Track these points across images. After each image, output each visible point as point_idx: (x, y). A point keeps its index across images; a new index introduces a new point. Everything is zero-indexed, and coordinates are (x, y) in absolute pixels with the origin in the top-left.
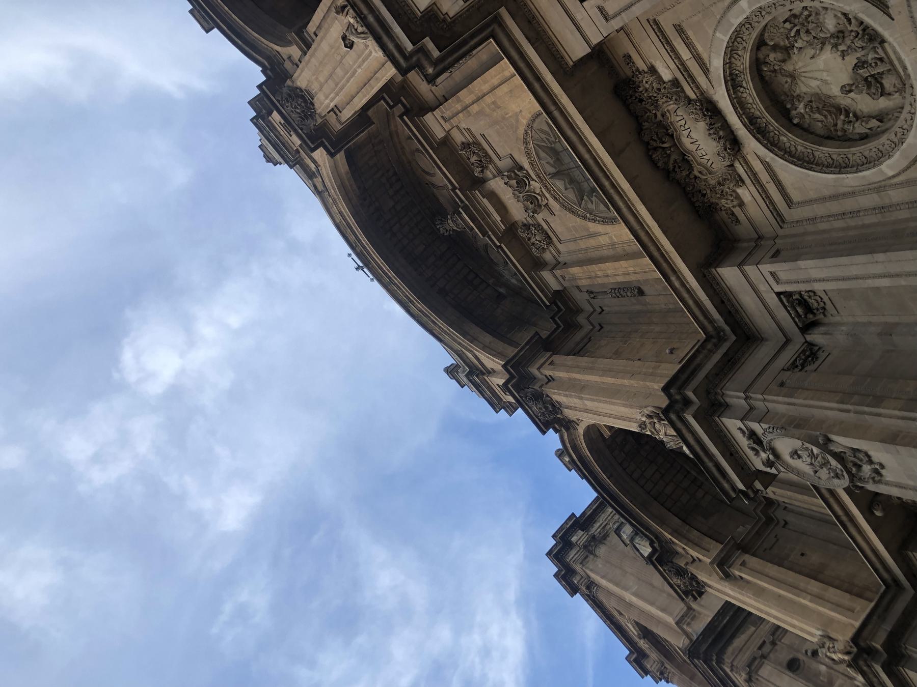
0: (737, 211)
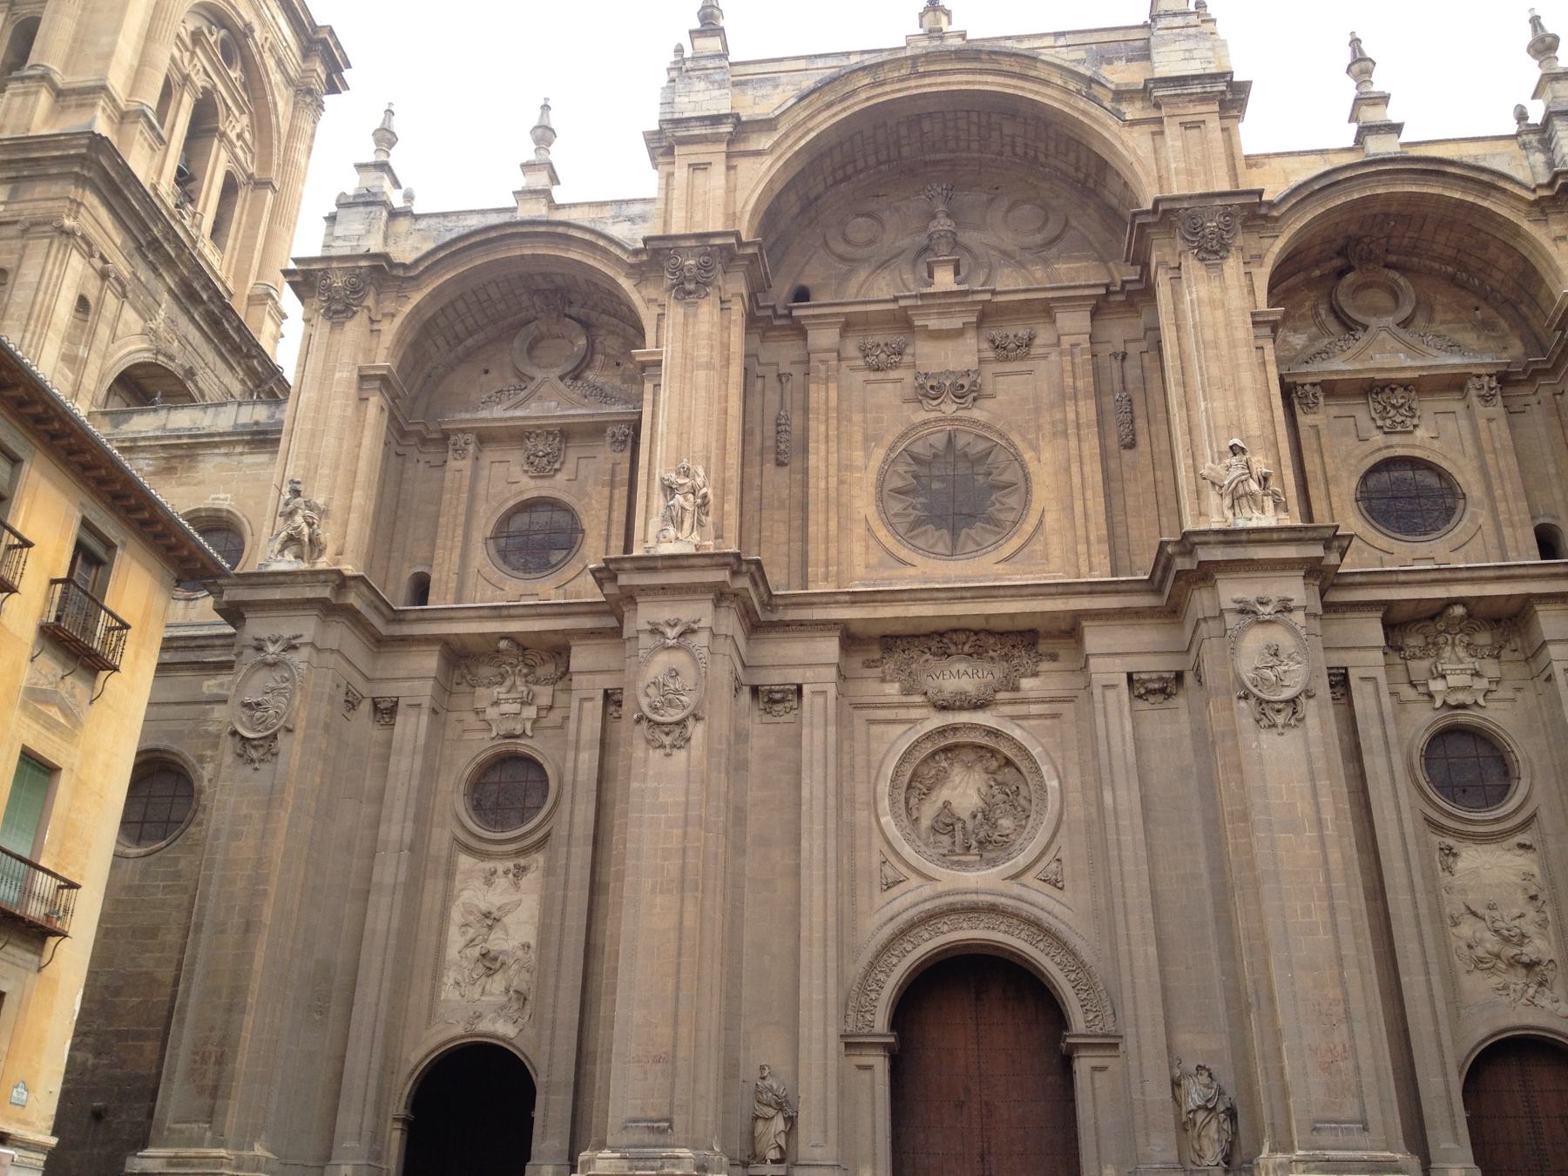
0: (878, 672)
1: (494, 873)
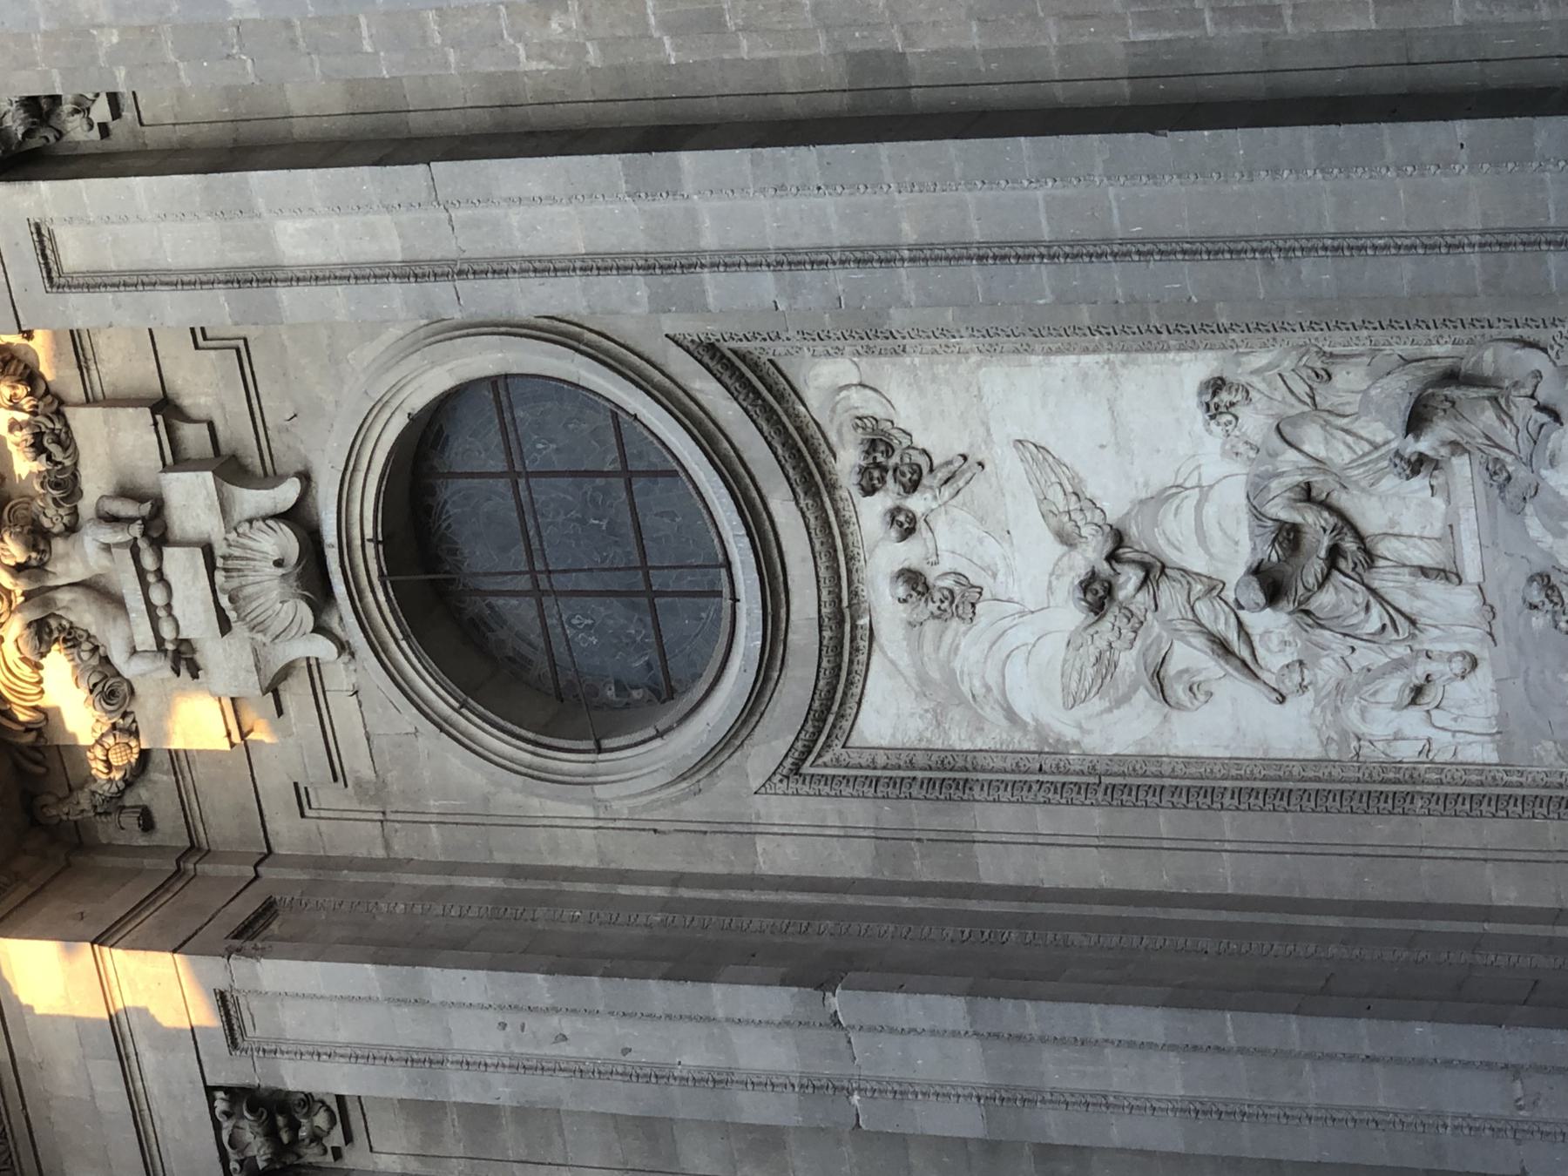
1: (914, 580)
